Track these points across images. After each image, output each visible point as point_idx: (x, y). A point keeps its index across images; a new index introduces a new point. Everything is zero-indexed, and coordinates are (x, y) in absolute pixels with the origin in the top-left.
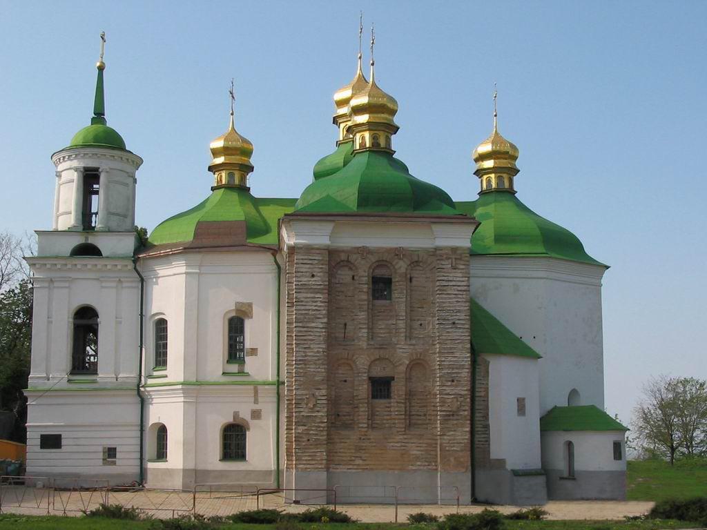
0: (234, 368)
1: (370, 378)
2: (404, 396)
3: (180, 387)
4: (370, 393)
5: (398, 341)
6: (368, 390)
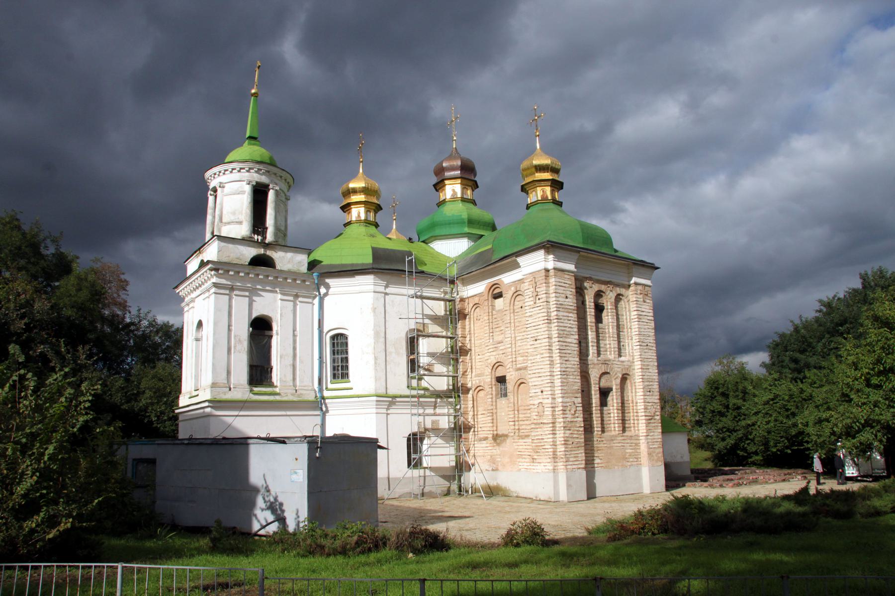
0: (414, 383)
1: (600, 388)
3: (375, 398)
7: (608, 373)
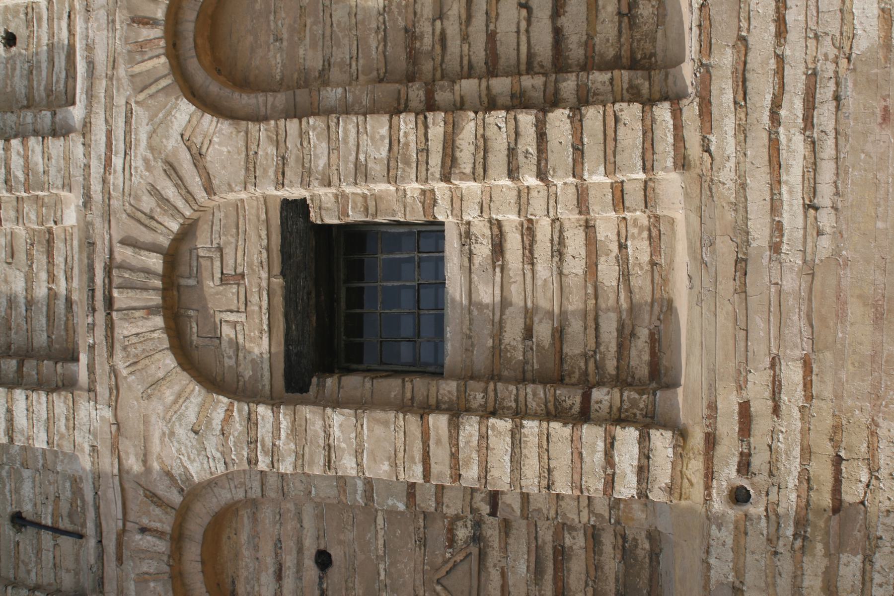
2: (406, 123)
4: (392, 386)
5: (67, 186)
6: (360, 405)
7: (177, 254)
